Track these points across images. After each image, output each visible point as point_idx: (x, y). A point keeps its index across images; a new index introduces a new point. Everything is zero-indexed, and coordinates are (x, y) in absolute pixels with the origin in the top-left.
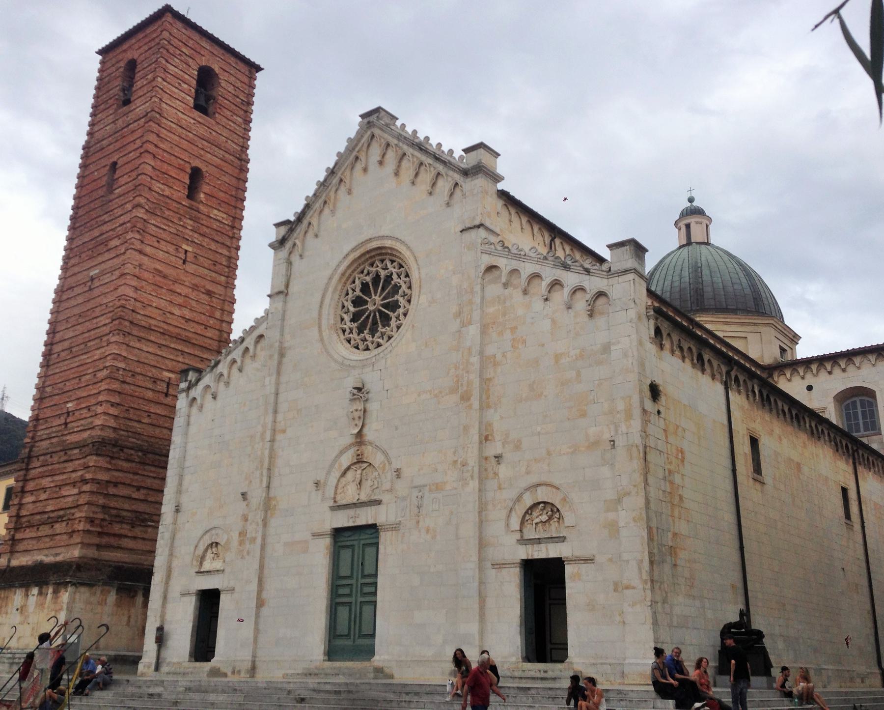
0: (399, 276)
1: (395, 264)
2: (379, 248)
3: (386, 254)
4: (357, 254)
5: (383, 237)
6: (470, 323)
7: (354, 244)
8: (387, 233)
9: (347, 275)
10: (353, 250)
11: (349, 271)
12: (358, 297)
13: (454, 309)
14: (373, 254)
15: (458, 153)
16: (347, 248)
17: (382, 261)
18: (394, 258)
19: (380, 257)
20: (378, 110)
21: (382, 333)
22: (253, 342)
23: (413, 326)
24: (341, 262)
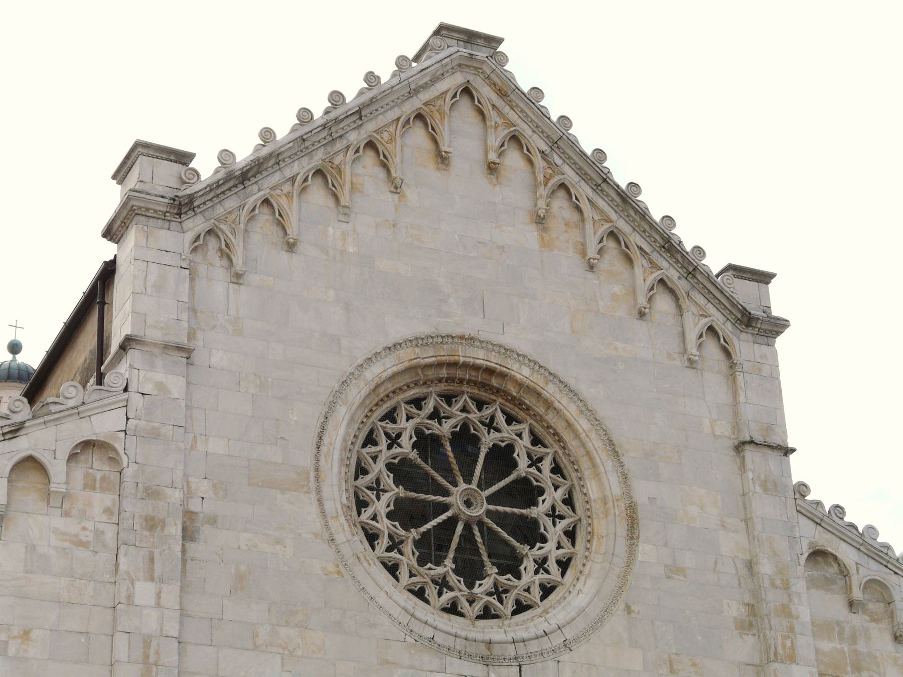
0: (535, 462)
1: (524, 428)
2: (490, 371)
3: (498, 391)
4: (428, 356)
5: (507, 351)
6: (792, 658)
7: (423, 329)
8: (524, 348)
9: (382, 392)
10: (418, 341)
11: (390, 387)
12: (405, 461)
13: (734, 610)
14: (459, 374)
15: (714, 263)
16: (400, 331)
17: (480, 405)
18: (521, 415)
19: (442, 387)
20: (493, 42)
21: (495, 585)
22: (63, 454)
23: (628, 609)
24: (377, 354)
